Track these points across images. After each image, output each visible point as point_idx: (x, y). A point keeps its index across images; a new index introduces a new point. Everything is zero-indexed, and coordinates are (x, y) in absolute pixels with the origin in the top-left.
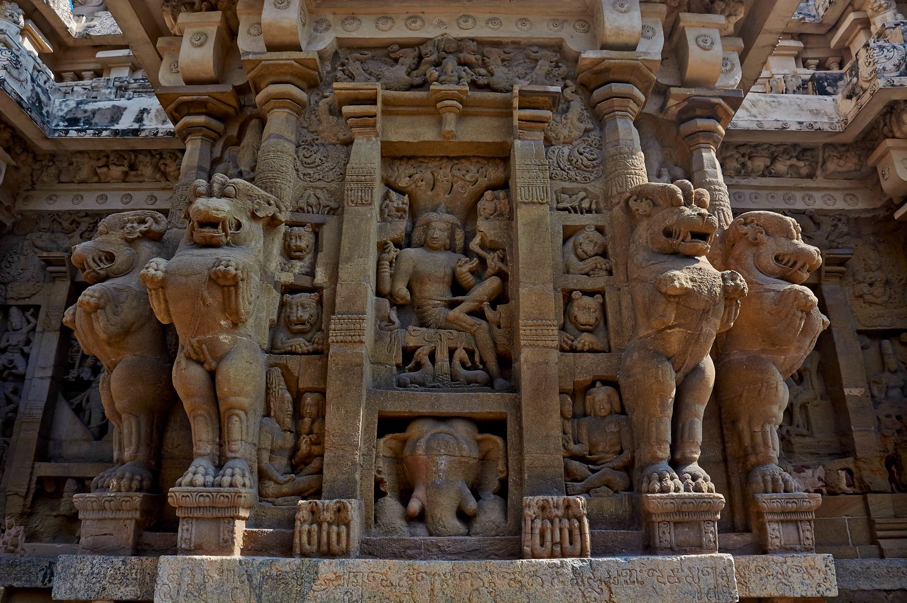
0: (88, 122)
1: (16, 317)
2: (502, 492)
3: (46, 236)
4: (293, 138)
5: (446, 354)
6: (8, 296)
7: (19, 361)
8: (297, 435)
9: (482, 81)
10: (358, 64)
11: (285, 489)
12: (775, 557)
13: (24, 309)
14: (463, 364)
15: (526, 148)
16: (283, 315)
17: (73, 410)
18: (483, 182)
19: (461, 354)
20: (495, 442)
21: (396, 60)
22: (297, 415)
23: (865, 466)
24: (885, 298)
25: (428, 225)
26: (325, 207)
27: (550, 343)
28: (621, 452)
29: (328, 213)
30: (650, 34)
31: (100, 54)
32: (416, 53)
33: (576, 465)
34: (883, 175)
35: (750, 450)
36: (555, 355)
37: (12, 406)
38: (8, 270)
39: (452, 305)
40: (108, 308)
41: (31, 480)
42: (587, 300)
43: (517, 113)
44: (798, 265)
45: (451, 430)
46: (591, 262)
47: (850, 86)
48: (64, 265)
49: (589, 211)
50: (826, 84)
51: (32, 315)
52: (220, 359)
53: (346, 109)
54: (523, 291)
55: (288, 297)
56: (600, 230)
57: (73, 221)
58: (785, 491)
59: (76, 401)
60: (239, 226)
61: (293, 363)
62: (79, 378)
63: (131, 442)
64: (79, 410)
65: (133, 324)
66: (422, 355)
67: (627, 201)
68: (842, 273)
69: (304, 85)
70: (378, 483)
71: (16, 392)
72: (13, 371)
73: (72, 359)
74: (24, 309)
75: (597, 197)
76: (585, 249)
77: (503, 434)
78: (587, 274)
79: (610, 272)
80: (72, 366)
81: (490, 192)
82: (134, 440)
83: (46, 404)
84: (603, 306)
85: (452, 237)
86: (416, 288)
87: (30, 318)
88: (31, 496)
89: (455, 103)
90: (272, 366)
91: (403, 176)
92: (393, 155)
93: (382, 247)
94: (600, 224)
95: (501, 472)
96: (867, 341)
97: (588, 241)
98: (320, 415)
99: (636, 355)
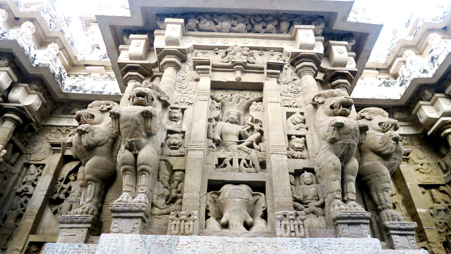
0: (81, 88)
1: (33, 168)
2: (265, 216)
3: (53, 135)
4: (175, 78)
5: (237, 161)
7: (31, 188)
8: (171, 190)
9: (251, 61)
10: (202, 54)
11: (164, 211)
12: (399, 251)
13: (37, 165)
14: (245, 165)
15: (270, 85)
16: (167, 142)
17: (53, 213)
18: (252, 99)
19: (244, 161)
20: (260, 195)
21: (217, 54)
22: (170, 181)
23: (433, 245)
24: (429, 171)
25: (229, 113)
26: (187, 103)
27: (283, 153)
28: (318, 200)
29: (189, 105)
30: (318, 47)
31: (88, 68)
32: (225, 51)
33: (297, 204)
34: (420, 116)
35: (378, 203)
36: (286, 158)
38: (33, 148)
39: (239, 143)
40: (90, 134)
41: (25, 243)
42: (298, 138)
43: (266, 71)
44: (390, 126)
45: (241, 188)
46: (298, 126)
47: (401, 81)
49: (296, 107)
50: (390, 84)
52: (139, 150)
53: (197, 67)
54: (271, 133)
55: (169, 135)
56: (302, 114)
57: (67, 130)
58: (399, 220)
59: (54, 209)
60: (153, 100)
61: (171, 160)
63: (90, 194)
64: (55, 213)
65: (99, 142)
66: (227, 161)
67: (313, 100)
68: (408, 159)
69: (180, 60)
70: (207, 211)
71: (26, 202)
72: (26, 193)
73: (56, 190)
74: (37, 165)
75: (300, 102)
76: (296, 120)
77: (264, 192)
78: (297, 130)
79: (307, 129)
80: (56, 193)
81: (255, 102)
82: (92, 193)
83: (41, 207)
84: (305, 143)
85: (239, 119)
86: (224, 137)
88: (24, 251)
89: (241, 67)
90: (161, 160)
91: (219, 94)
92: (216, 86)
93: (210, 120)
94: (302, 112)
95: (263, 207)
96: (423, 189)
97: (296, 117)
98: (181, 181)
99: (322, 156)
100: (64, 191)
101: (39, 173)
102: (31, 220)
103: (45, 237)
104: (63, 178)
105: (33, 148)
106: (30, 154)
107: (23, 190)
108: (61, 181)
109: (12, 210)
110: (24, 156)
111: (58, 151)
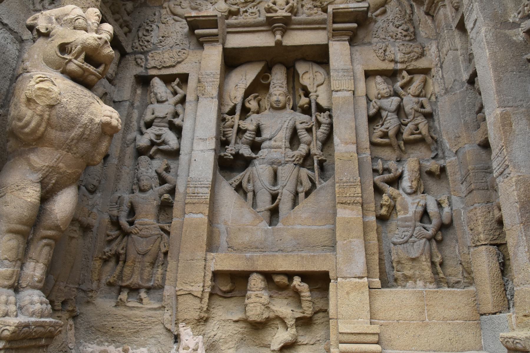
13: (167, 80)
37: (166, 186)
38: (147, 38)
48: (217, 28)
51: (178, 85)
72: (161, 147)
87: (176, 87)
100: (248, 136)
101: (178, 97)
102: (200, 216)
103: (248, 259)
104: (234, 107)
105: (147, 38)
106: (145, 53)
107: (151, 141)
108: (232, 112)
109: (142, 191)
110: (131, 58)
111: (212, 39)
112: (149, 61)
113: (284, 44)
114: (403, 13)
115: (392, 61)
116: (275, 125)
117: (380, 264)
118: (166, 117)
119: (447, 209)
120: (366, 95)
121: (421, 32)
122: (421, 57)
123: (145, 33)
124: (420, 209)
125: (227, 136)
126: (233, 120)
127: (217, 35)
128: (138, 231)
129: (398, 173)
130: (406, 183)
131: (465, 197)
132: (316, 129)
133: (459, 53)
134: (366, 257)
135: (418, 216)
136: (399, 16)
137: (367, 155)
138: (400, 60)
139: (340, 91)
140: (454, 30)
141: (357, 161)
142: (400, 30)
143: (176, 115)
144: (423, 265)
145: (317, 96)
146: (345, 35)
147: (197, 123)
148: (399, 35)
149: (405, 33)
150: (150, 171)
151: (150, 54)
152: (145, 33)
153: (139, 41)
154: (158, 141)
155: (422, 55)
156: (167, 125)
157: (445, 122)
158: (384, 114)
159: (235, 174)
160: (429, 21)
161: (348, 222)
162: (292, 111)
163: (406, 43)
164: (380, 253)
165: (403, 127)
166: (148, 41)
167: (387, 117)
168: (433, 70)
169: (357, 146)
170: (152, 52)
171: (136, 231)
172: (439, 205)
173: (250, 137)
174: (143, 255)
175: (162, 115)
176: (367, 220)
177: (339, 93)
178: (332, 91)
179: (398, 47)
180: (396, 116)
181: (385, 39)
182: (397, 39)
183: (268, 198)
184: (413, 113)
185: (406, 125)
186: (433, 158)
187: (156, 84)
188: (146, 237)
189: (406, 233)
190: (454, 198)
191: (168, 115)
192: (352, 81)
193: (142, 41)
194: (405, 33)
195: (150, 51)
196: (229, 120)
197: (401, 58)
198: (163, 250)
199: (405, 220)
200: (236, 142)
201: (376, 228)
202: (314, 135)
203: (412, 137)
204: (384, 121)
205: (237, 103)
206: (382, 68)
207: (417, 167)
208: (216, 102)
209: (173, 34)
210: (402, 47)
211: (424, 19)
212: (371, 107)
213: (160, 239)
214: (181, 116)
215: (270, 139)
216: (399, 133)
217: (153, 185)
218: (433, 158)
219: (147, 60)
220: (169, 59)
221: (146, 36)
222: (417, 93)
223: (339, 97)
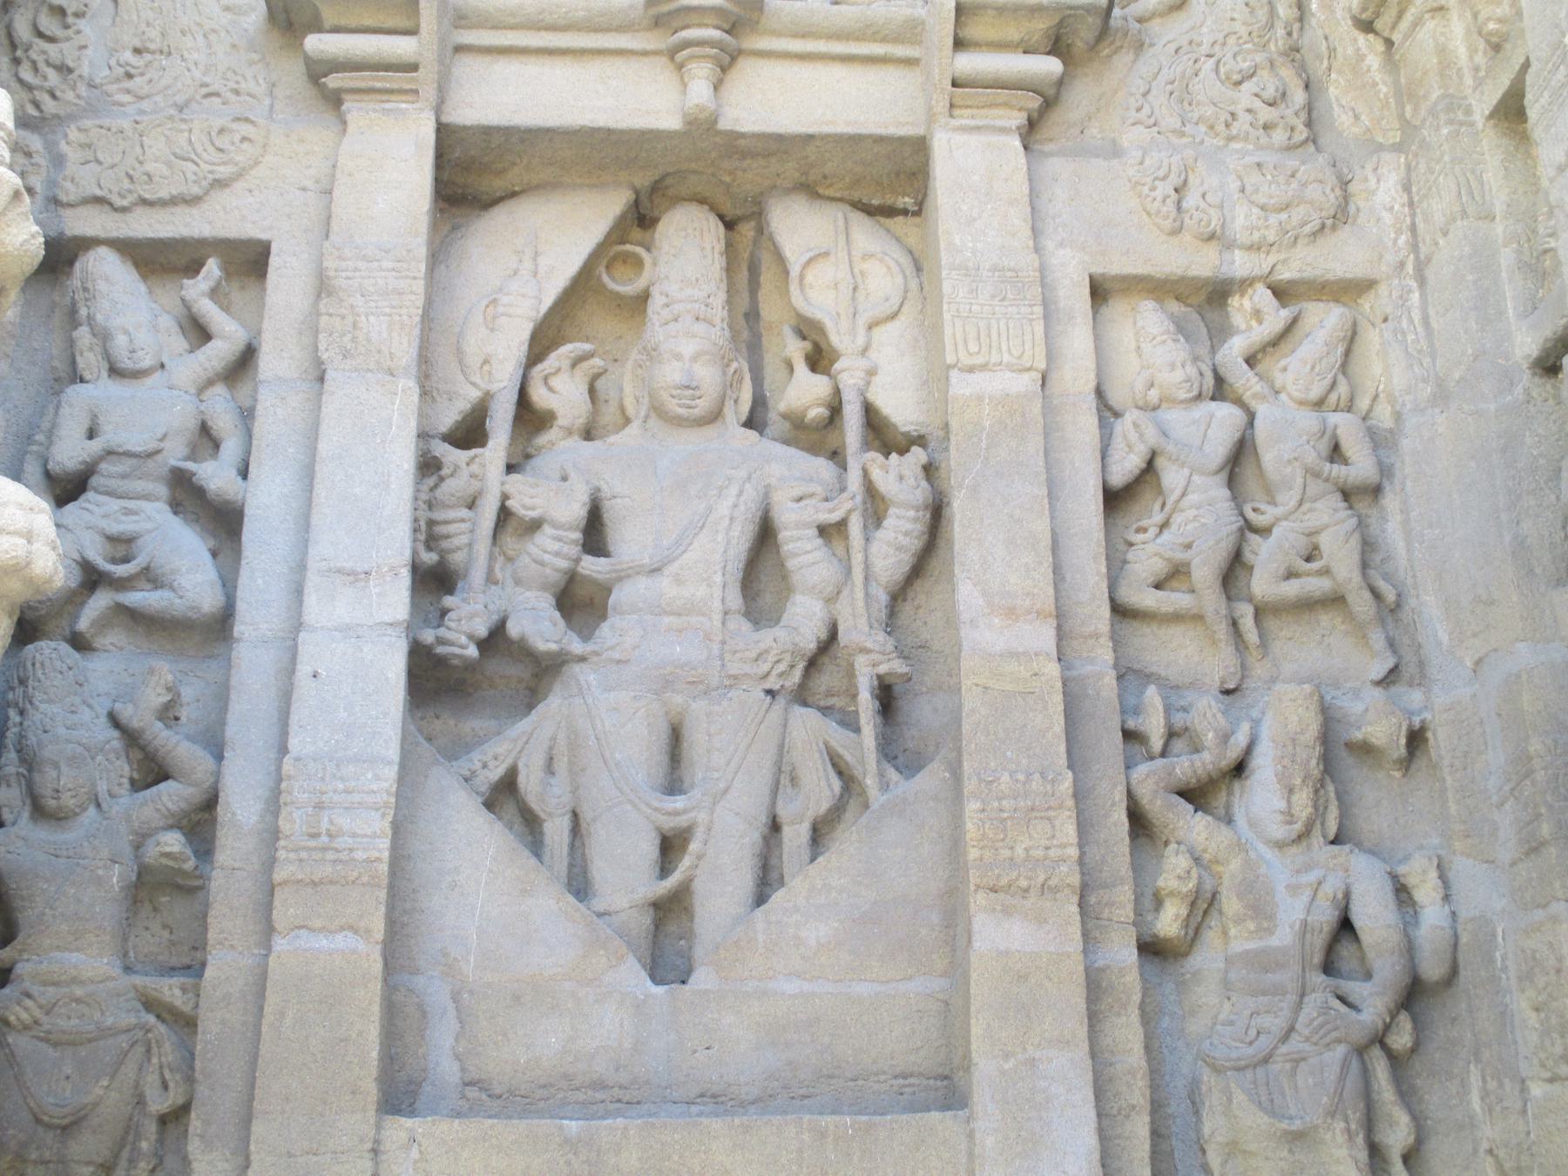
6: (69, 192)
13: (161, 261)
37: (170, 795)
48: (412, 32)
51: (214, 293)
62: (495, 640)
74: (161, 261)
87: (209, 310)
101: (219, 352)
102: (343, 941)
112: (71, 168)
113: (724, 124)
114: (1262, 15)
115: (1212, 237)
116: (680, 506)
117: (1156, 1155)
118: (158, 452)
119: (1432, 914)
120: (1099, 393)
121: (1337, 110)
122: (1334, 228)
123: (48, 24)
124: (1326, 917)
125: (445, 544)
126: (475, 468)
127: (413, 67)
128: (37, 1013)
129: (1233, 754)
130: (1265, 799)
131: (1513, 864)
132: (865, 527)
133: (1499, 229)
134: (1103, 1136)
135: (1319, 942)
136: (1243, 31)
137: (1099, 660)
138: (1243, 237)
139: (984, 367)
140: (1480, 126)
141: (1059, 698)
142: (1245, 97)
143: (206, 438)
144: (1338, 1162)
145: (872, 372)
146: (1006, 105)
147: (320, 491)
148: (1244, 118)
149: (1266, 114)
150: (86, 715)
151: (73, 134)
152: (48, 24)
153: (16, 61)
154: (121, 570)
155: (1341, 215)
156: (163, 490)
157: (1431, 526)
158: (1172, 477)
159: (474, 724)
160: (1374, 61)
161: (1022, 978)
162: (752, 435)
163: (1269, 158)
164: (1157, 1107)
165: (1254, 539)
166: (64, 69)
167: (1183, 495)
168: (1383, 289)
169: (1059, 628)
170: (88, 123)
171: (24, 1016)
172: (1402, 892)
173: (557, 554)
174: (64, 1128)
175: (136, 440)
176: (1100, 963)
177: (977, 377)
178: (949, 367)
179: (1240, 178)
180: (1226, 493)
181: (1182, 134)
182: (1230, 139)
183: (648, 848)
184: (1299, 481)
185: (1264, 531)
186: (1378, 683)
187: (102, 286)
188: (73, 1044)
189: (1266, 1021)
190: (1464, 868)
191: (166, 445)
192: (1039, 328)
193: (34, 63)
194: (1266, 114)
195: (72, 117)
196: (456, 468)
197: (1252, 229)
198: (159, 1103)
199: (1263, 961)
200: (490, 579)
201: (1137, 998)
202: (857, 559)
203: (1292, 589)
204: (1174, 511)
205: (494, 387)
206: (1167, 270)
207: (1314, 729)
208: (408, 387)
209: (188, 41)
210: (1253, 178)
211: (1350, 51)
212: (1118, 443)
213: (140, 1049)
214: (231, 448)
215: (655, 571)
216: (1234, 569)
217: (102, 787)
218: (1378, 683)
219: (58, 161)
220: (169, 164)
221: (51, 40)
222: (1315, 392)
223: (980, 398)
